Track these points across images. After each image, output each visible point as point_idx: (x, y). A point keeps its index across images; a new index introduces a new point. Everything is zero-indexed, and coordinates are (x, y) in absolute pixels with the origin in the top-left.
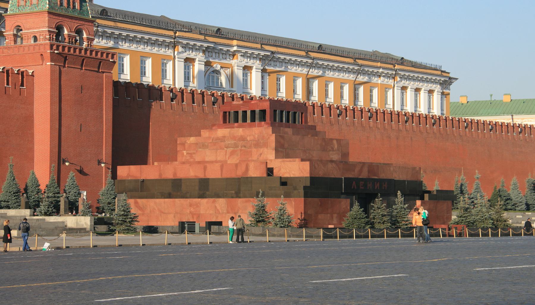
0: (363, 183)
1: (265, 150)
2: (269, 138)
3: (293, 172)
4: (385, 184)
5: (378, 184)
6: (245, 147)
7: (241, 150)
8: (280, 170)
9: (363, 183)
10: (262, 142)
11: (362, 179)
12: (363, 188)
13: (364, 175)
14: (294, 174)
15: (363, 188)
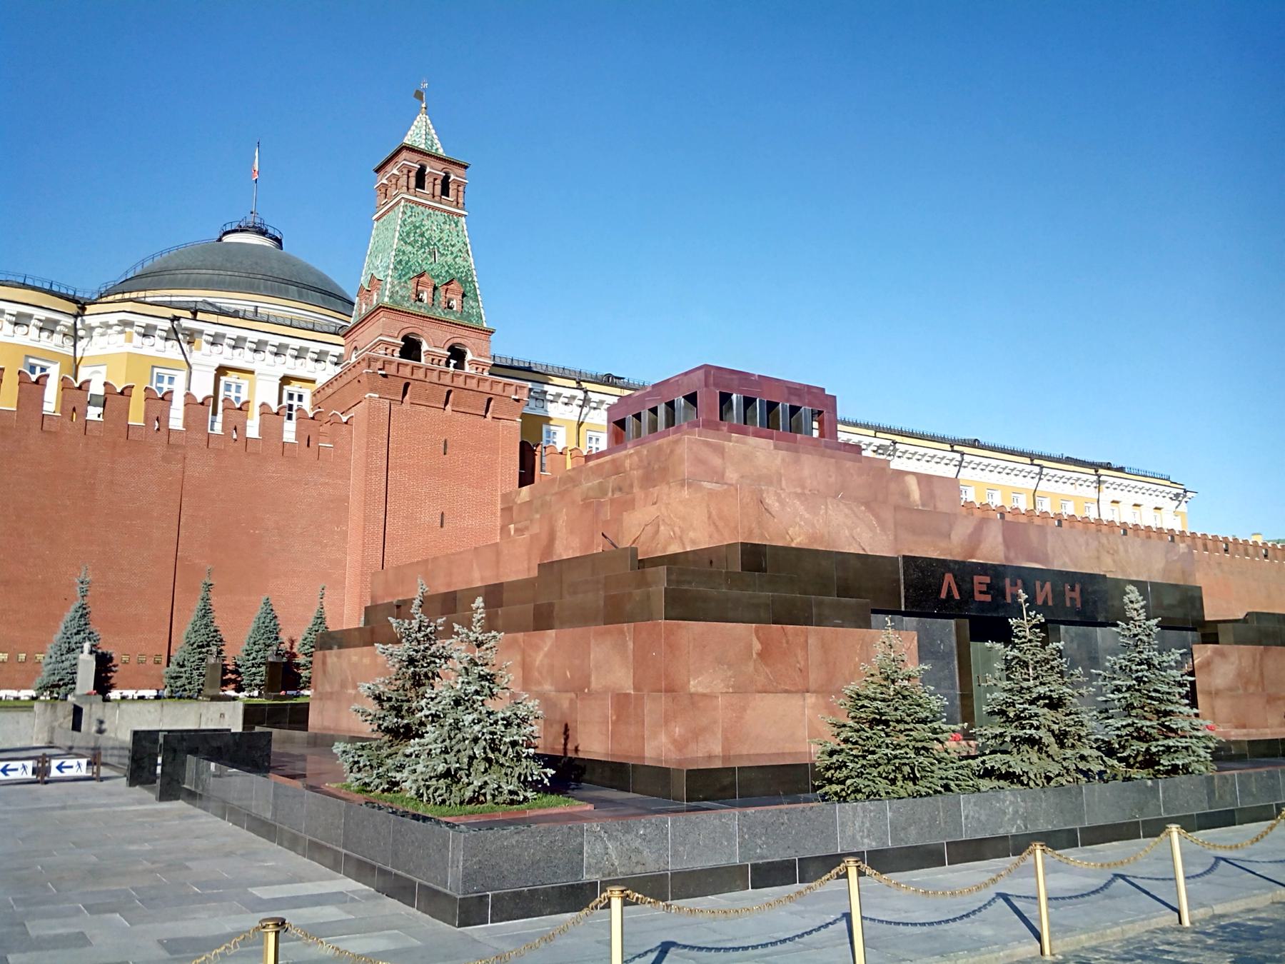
0: (987, 580)
1: (665, 488)
2: (672, 451)
3: (692, 534)
4: (1073, 589)
5: (1048, 586)
6: (620, 489)
7: (612, 500)
8: (657, 532)
9: (987, 580)
10: (656, 467)
11: (984, 569)
12: (988, 598)
13: (992, 551)
14: (693, 542)
15: (988, 598)
